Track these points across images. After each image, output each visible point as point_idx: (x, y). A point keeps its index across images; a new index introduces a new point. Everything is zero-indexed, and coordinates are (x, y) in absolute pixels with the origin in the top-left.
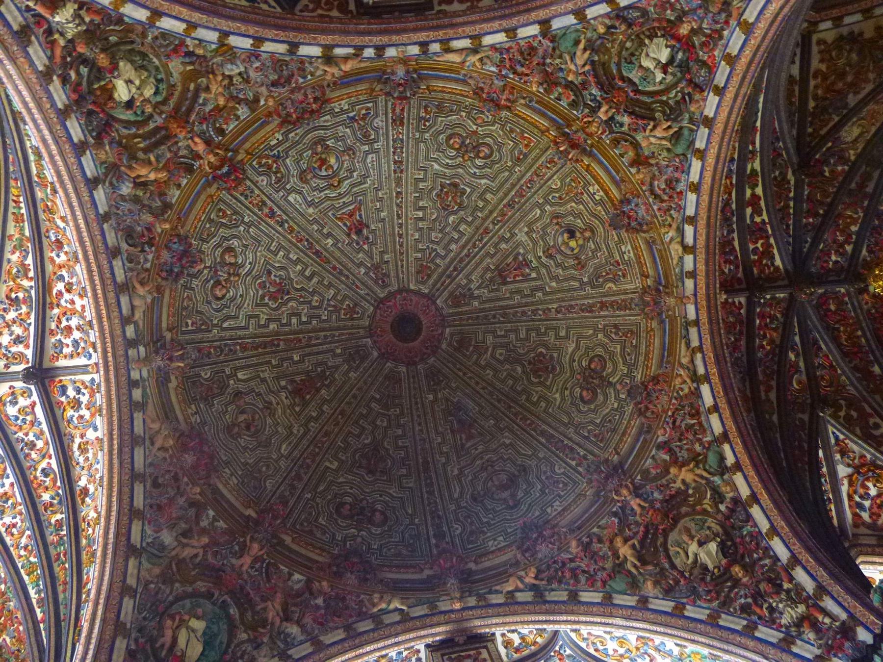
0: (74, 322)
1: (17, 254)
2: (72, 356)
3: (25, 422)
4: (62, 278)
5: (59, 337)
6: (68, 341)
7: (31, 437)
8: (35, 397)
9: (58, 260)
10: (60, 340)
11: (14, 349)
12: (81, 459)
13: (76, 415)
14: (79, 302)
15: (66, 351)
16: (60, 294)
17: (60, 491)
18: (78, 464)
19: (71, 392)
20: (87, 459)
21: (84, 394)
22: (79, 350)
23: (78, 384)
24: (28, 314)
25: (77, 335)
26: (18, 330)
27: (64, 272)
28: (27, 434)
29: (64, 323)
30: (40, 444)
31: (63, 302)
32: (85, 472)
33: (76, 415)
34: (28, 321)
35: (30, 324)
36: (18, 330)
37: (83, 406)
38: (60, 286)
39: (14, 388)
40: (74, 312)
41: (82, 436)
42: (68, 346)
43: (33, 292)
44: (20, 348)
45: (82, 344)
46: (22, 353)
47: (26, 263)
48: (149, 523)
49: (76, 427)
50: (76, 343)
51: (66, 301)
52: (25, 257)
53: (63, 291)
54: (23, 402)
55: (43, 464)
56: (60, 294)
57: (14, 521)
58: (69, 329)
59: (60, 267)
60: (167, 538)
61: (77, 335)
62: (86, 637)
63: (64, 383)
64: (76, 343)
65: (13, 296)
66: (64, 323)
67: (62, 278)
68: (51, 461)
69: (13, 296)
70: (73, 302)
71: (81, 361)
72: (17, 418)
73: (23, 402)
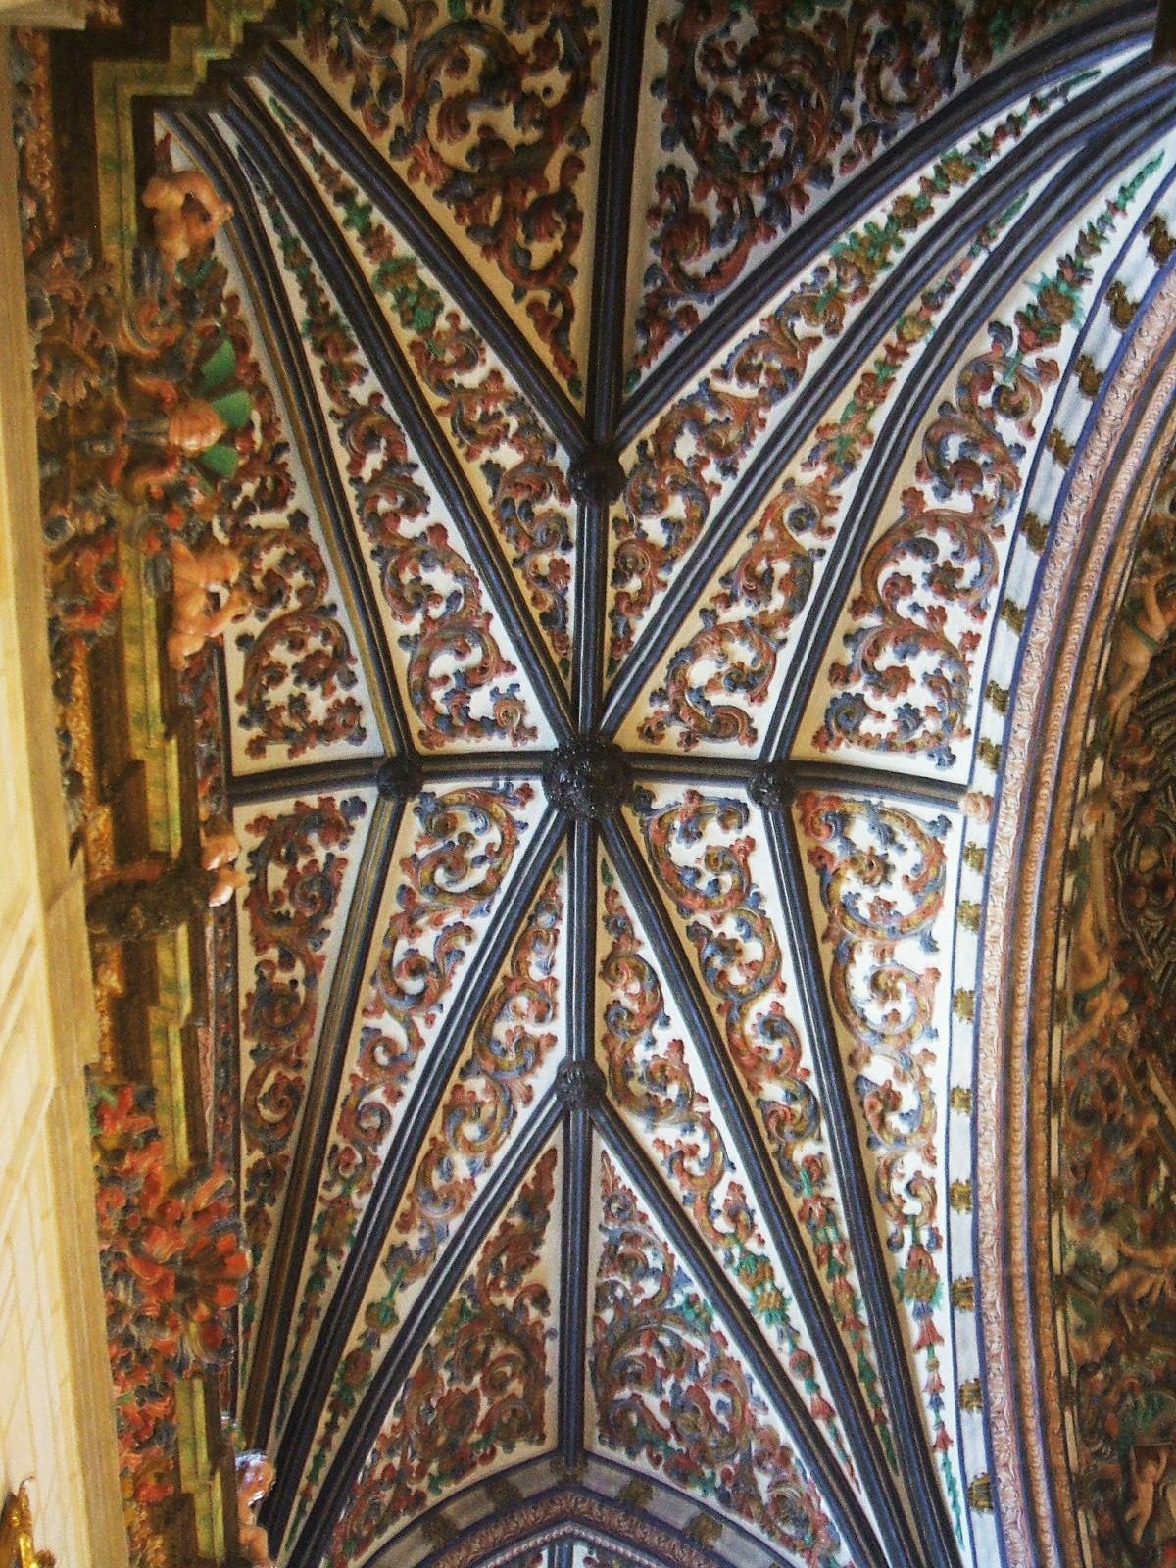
0: (924, 662)
1: (821, 469)
2: (889, 745)
3: (716, 884)
4: (926, 549)
5: (855, 688)
6: (888, 705)
7: (730, 928)
8: (756, 826)
9: (932, 502)
10: (860, 697)
11: (718, 698)
12: (875, 1012)
13: (868, 895)
14: (957, 622)
15: (868, 726)
16: (902, 585)
17: (812, 1083)
18: (864, 1020)
19: (862, 833)
20: (895, 1015)
21: (902, 848)
22: (918, 735)
23: (887, 820)
24: (789, 614)
25: (919, 696)
26: (742, 652)
27: (944, 541)
28: (719, 921)
29: (886, 659)
30: (754, 950)
31: (903, 607)
32: (889, 1047)
33: (868, 895)
34: (780, 634)
35: (783, 642)
36: (742, 652)
37: (896, 878)
38: (913, 566)
39: (701, 797)
40: (932, 638)
41: (882, 953)
42: (881, 716)
43: (820, 567)
44: (739, 699)
45: (931, 725)
46: (741, 712)
47: (834, 492)
48: (1072, 1212)
49: (864, 926)
50: (910, 716)
51: (916, 607)
52: (838, 480)
53: (919, 580)
54: (716, 835)
55: (762, 1006)
56: (902, 585)
57: (688, 1139)
58: (897, 679)
59: (935, 520)
60: (1105, 1248)
61: (919, 696)
62: (320, 1127)
63: (848, 807)
64: (910, 716)
65: (762, 567)
66: (886, 659)
67: (926, 549)
68: (783, 1000)
69: (762, 567)
70: (937, 615)
71: (920, 765)
72: (698, 875)
73: (716, 835)
